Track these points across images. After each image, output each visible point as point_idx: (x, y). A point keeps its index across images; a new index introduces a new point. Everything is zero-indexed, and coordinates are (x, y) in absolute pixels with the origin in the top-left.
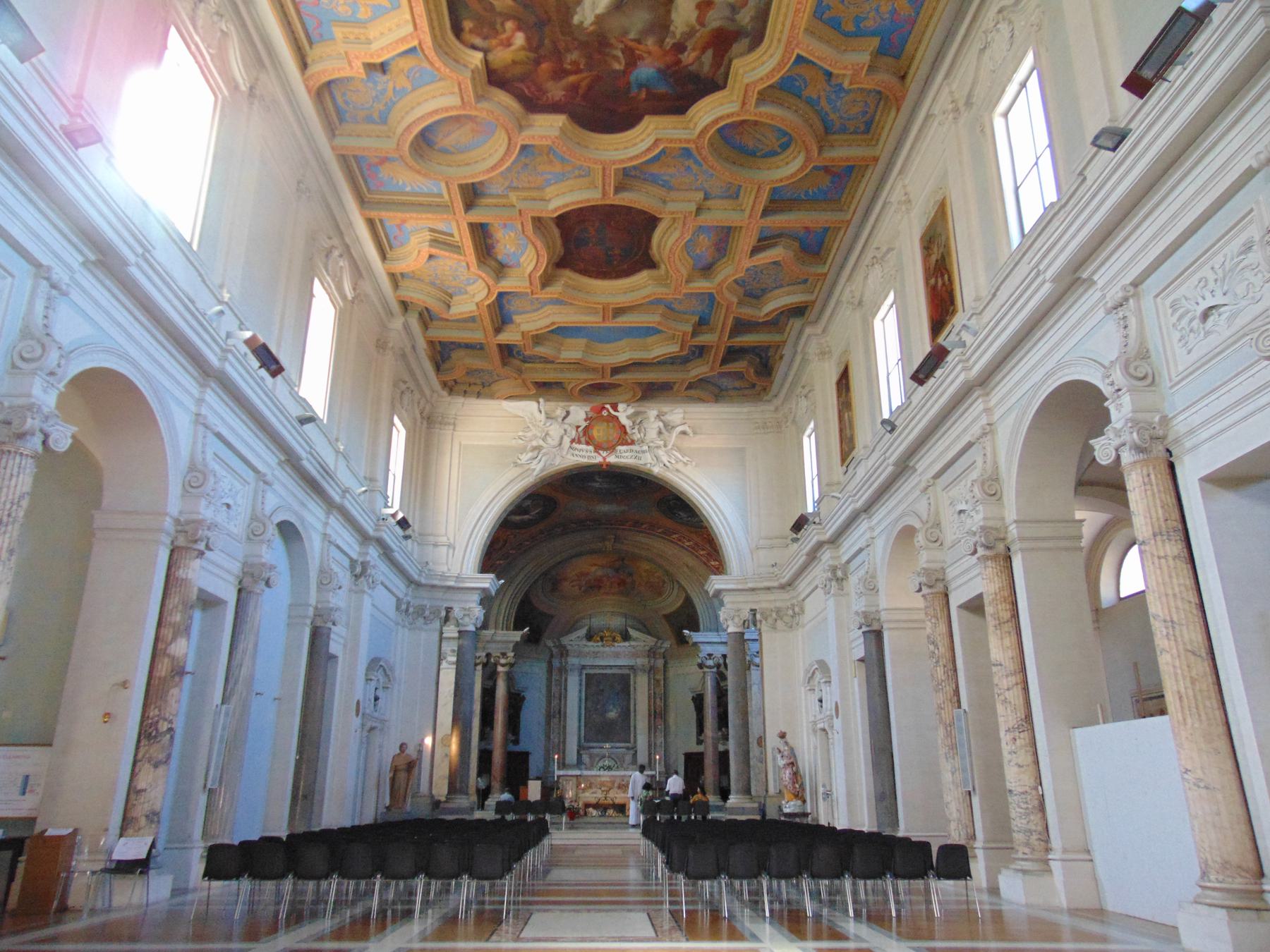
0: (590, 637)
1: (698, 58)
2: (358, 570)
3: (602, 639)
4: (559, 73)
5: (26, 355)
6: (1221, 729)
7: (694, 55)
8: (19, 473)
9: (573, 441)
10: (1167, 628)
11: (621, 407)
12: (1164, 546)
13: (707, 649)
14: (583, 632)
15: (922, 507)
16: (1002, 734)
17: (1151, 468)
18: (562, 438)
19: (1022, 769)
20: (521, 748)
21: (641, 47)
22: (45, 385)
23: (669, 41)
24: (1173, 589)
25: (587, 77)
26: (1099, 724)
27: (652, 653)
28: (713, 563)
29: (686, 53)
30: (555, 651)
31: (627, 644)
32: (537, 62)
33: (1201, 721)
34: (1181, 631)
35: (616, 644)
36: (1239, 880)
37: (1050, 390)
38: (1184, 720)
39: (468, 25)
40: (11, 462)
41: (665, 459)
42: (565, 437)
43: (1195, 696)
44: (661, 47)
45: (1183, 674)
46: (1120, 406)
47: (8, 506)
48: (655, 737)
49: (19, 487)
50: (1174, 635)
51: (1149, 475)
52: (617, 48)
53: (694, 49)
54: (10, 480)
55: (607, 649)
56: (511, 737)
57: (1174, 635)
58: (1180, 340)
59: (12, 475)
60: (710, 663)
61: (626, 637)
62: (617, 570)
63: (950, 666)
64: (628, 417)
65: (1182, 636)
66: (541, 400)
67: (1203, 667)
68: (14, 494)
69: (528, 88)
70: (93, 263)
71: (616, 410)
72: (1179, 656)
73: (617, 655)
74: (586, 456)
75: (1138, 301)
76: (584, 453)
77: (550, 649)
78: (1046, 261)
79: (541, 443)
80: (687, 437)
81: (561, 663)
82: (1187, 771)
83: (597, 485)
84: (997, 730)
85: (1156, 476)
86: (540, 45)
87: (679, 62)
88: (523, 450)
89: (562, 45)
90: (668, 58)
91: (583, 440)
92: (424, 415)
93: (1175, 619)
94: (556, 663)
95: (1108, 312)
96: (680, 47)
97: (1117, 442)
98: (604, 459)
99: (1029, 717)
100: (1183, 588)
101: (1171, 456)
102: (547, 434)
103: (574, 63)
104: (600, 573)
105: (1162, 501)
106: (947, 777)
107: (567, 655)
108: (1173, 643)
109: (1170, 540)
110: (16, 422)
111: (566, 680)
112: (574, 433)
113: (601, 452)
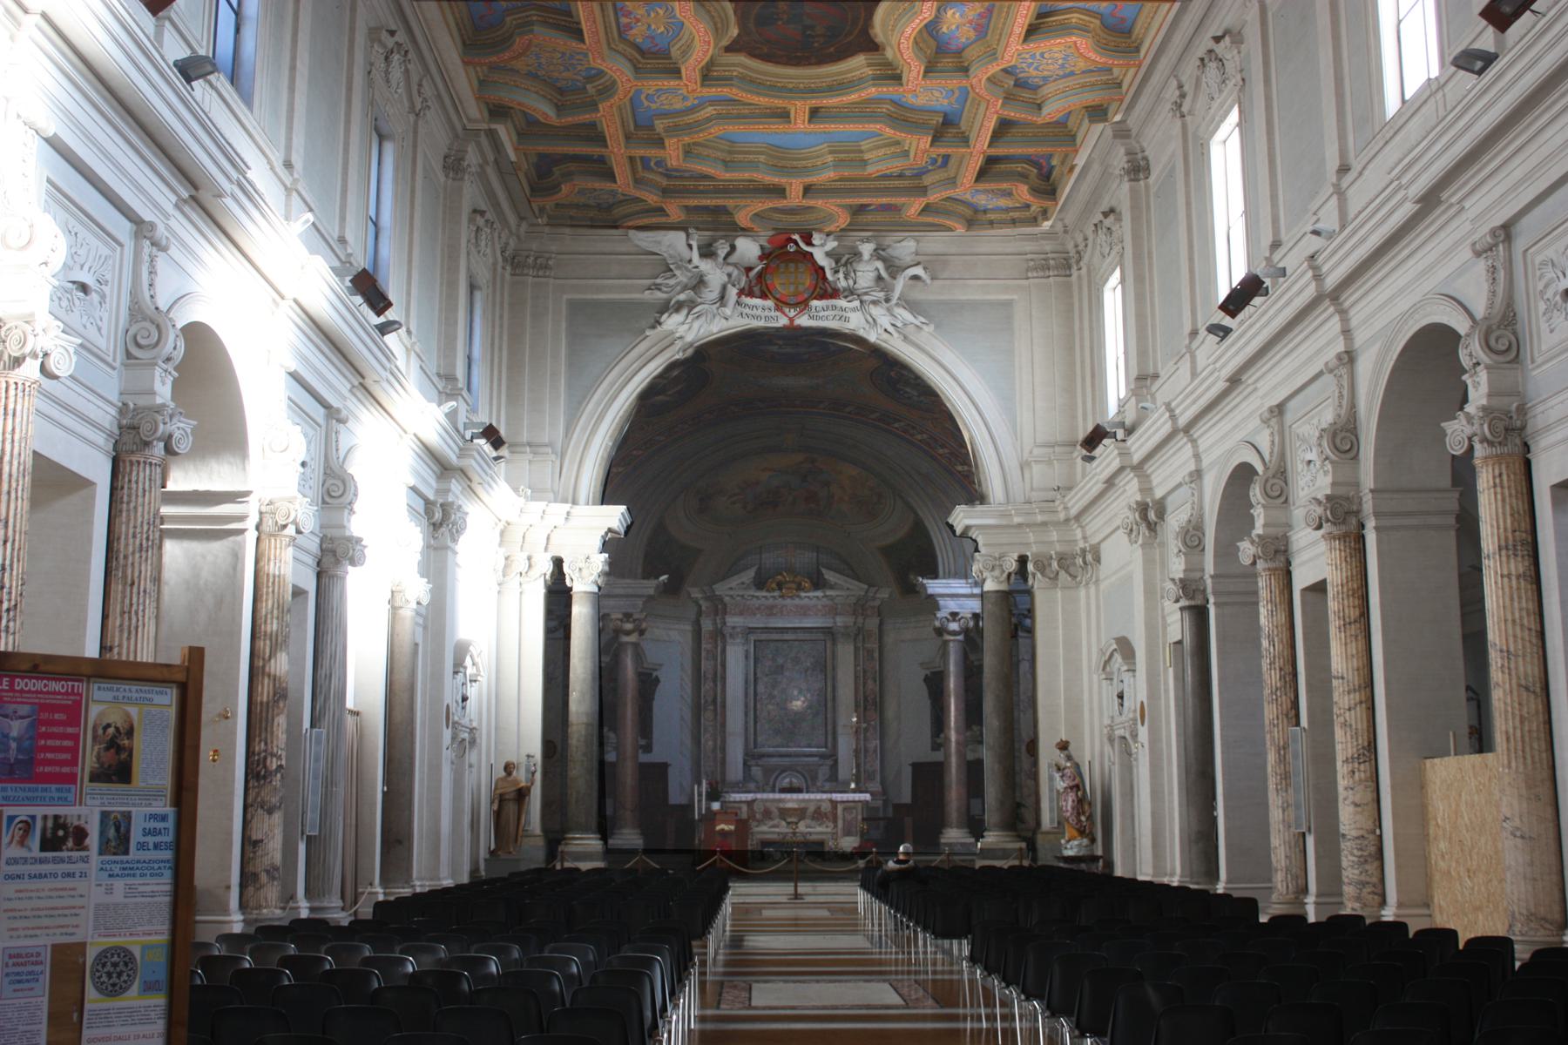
0: (760, 583)
2: (438, 515)
3: (780, 586)
5: (139, 338)
6: (1546, 774)
8: (151, 488)
9: (741, 293)
10: (1502, 658)
11: (817, 239)
12: (1508, 562)
13: (950, 606)
14: (751, 573)
15: (1264, 441)
16: (1339, 764)
17: (1503, 466)
18: (724, 288)
19: (1359, 809)
20: (656, 756)
22: (163, 375)
24: (1513, 613)
26: (1450, 755)
27: (859, 607)
28: (960, 468)
30: (704, 605)
31: (819, 593)
33: (1525, 764)
34: (1516, 662)
35: (803, 594)
36: (1542, 932)
37: (1410, 334)
38: (1509, 762)
40: (141, 475)
41: (885, 321)
42: (729, 286)
43: (1522, 737)
45: (1513, 714)
46: (1477, 385)
47: (145, 528)
48: (866, 739)
49: (152, 504)
50: (1509, 668)
51: (1500, 475)
54: (144, 495)
55: (788, 601)
56: (643, 742)
57: (1509, 668)
58: (1544, 314)
59: (144, 491)
60: (954, 626)
61: (819, 583)
63: (1288, 669)
64: (828, 254)
65: (1517, 668)
67: (1534, 704)
68: (149, 513)
70: (185, 201)
71: (809, 244)
72: (1511, 692)
73: (804, 612)
74: (761, 315)
75: (1510, 243)
76: (759, 312)
77: (696, 602)
78: (1409, 176)
80: (919, 284)
81: (715, 623)
82: (1507, 818)
83: (775, 348)
84: (1334, 759)
85: (1508, 476)
88: (665, 308)
91: (756, 290)
93: (1512, 649)
94: (707, 625)
95: (1478, 254)
97: (1468, 430)
98: (791, 320)
99: (1372, 746)
100: (1524, 614)
101: (1529, 452)
105: (1512, 507)
106: (1276, 815)
108: (1507, 676)
109: (1516, 555)
110: (145, 428)
111: (724, 651)
113: (787, 310)
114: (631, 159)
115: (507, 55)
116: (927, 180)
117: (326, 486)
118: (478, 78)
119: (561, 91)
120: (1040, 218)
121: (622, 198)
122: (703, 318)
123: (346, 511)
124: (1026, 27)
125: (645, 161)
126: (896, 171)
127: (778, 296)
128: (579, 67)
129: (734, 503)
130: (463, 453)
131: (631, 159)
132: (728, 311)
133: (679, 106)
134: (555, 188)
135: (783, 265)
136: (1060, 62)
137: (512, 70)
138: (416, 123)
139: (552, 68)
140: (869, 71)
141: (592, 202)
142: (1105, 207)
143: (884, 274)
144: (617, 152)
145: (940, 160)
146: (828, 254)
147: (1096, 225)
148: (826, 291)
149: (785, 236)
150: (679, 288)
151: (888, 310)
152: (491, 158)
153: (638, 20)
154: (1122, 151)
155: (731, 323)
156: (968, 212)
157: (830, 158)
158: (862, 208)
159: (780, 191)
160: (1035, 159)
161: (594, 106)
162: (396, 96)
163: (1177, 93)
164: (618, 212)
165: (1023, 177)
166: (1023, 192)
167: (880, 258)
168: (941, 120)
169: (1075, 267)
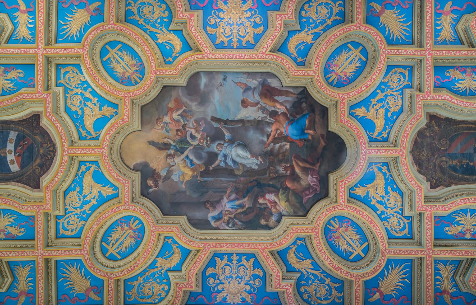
1: (281, 104)
7: (278, 106)
23: (268, 119)
25: (297, 164)
29: (278, 110)
32: (287, 188)
39: (263, 222)
44: (272, 124)
52: (274, 147)
69: (307, 195)
86: (273, 186)
87: (284, 114)
90: (281, 120)
96: (274, 114)
103: (286, 169)
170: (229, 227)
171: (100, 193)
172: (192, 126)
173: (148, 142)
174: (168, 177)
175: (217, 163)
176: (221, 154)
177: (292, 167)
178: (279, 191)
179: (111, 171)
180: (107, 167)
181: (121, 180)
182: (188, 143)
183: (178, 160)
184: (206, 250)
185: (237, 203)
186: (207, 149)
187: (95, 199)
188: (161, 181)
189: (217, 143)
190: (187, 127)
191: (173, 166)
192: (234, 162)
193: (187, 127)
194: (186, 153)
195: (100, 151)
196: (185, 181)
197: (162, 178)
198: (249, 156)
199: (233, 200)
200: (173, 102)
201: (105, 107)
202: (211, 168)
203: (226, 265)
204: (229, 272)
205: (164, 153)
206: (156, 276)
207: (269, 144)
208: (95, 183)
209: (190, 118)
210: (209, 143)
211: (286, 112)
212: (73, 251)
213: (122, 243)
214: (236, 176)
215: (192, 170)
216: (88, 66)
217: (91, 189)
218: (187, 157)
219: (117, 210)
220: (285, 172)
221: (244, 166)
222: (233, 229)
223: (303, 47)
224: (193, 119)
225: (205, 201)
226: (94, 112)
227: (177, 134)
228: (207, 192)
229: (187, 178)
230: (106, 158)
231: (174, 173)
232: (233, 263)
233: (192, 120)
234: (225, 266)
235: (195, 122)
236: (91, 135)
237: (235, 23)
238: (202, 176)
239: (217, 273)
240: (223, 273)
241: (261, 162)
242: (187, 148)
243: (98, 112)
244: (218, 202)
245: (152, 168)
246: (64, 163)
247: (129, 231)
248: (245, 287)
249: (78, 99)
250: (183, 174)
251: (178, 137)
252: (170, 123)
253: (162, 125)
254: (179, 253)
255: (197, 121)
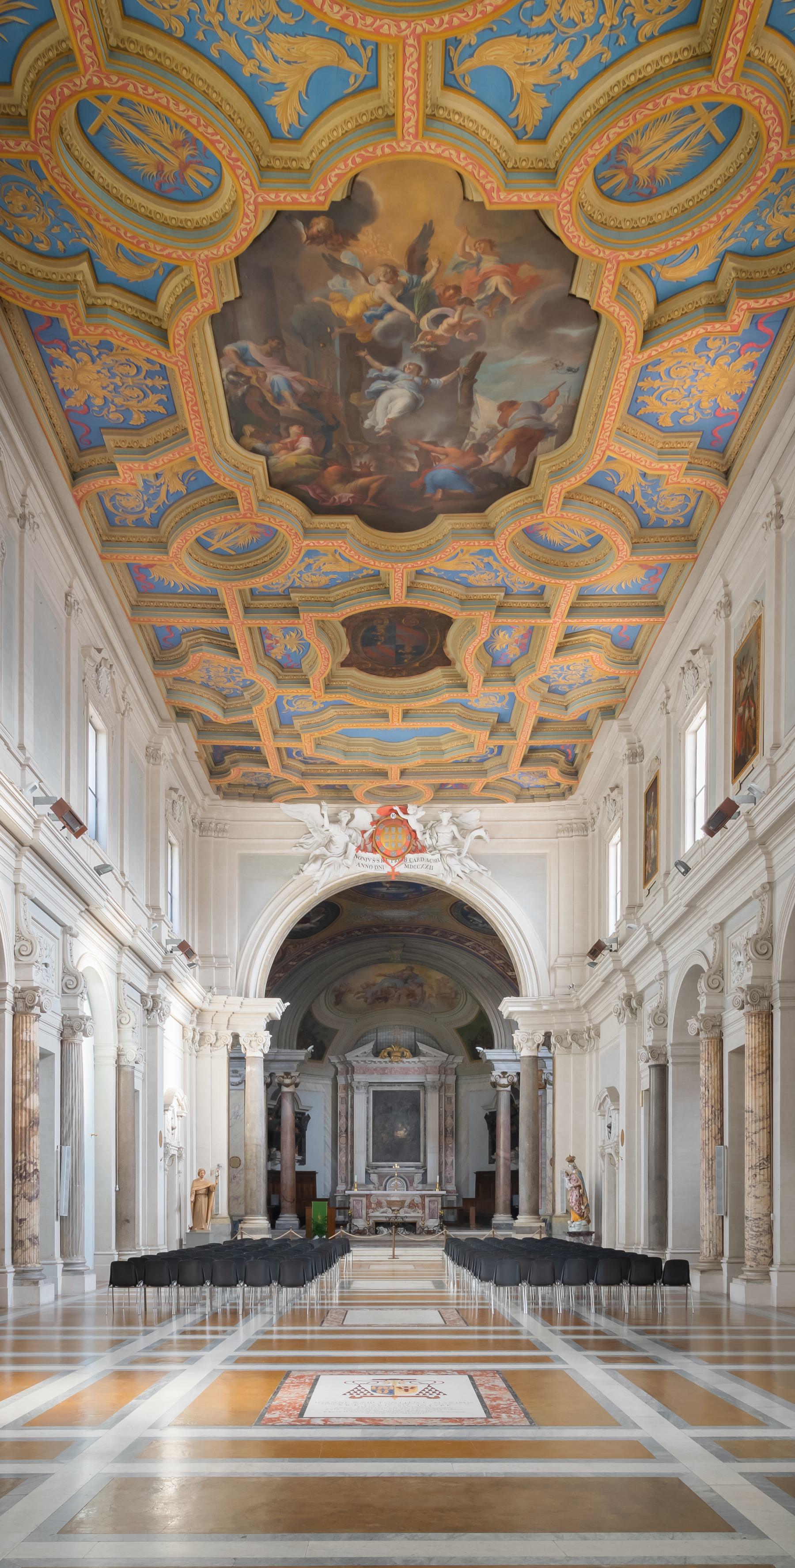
0: (376, 1053)
1: (500, 458)
3: (389, 1055)
4: (347, 477)
7: (494, 455)
9: (359, 848)
11: (411, 809)
18: (347, 845)
21: (438, 449)
23: (468, 443)
27: (442, 1070)
29: (487, 454)
30: (340, 1067)
31: (416, 1059)
32: (324, 465)
35: (405, 1060)
42: (350, 844)
44: (459, 448)
53: (495, 449)
55: (395, 1065)
61: (415, 1052)
62: (406, 981)
64: (419, 821)
66: (323, 803)
71: (405, 813)
73: (406, 1072)
76: (371, 863)
79: (322, 850)
81: (347, 1080)
83: (384, 890)
86: (328, 447)
88: (305, 860)
89: (351, 449)
91: (369, 847)
92: (196, 821)
96: (480, 448)
98: (393, 868)
102: (331, 841)
104: (386, 984)
107: (353, 1072)
112: (360, 839)
113: (389, 861)
114: (278, 749)
115: (184, 669)
116: (487, 765)
117: (65, 981)
118: (166, 687)
119: (226, 697)
120: (567, 793)
121: (274, 779)
122: (332, 867)
123: (79, 999)
124: (556, 646)
125: (289, 751)
126: (464, 758)
127: (384, 851)
128: (238, 679)
129: (359, 998)
130: (166, 960)
131: (278, 749)
132: (349, 862)
133: (310, 709)
134: (226, 772)
135: (387, 829)
136: (582, 673)
137: (190, 681)
138: (122, 720)
139: (218, 679)
140: (444, 681)
141: (254, 783)
142: (612, 785)
143: (458, 835)
144: (268, 745)
145: (496, 750)
146: (419, 821)
147: (605, 798)
148: (417, 847)
149: (389, 808)
150: (315, 846)
151: (460, 861)
152: (180, 749)
153: (277, 642)
154: (625, 741)
155: (352, 870)
156: (516, 789)
157: (418, 749)
158: (442, 787)
159: (384, 774)
160: (563, 749)
161: (249, 708)
162: (106, 699)
163: (665, 695)
164: (272, 789)
165: (555, 762)
166: (554, 774)
167: (455, 823)
168: (496, 719)
169: (590, 829)
170: (227, 374)
171: (280, 87)
172: (465, 317)
173: (431, 222)
174: (336, 266)
175: (377, 364)
176: (396, 372)
177: (369, 474)
178: (318, 456)
179: (349, 162)
180: (363, 152)
181: (325, 185)
182: (426, 311)
183: (382, 290)
184: (171, 358)
185: (286, 394)
186: (408, 348)
187: (258, 72)
188: (327, 252)
189: (423, 365)
190: (464, 308)
191: (367, 280)
192: (379, 393)
193: (464, 308)
194: (400, 307)
195: (409, 134)
196: (329, 303)
197: (335, 254)
198: (391, 416)
199: (290, 387)
200: (533, 274)
201: (544, 103)
202: (363, 354)
203: (139, 369)
204: (124, 373)
205: (399, 260)
206: (66, 225)
207: (417, 445)
208: (308, 74)
209: (486, 313)
210: (424, 350)
211: (482, 465)
212: (87, 41)
213: (136, 141)
214: (347, 394)
215: (358, 319)
216: (673, 95)
217: (288, 62)
218: (390, 309)
219: (239, 172)
220: (358, 464)
221: (371, 407)
222: (223, 381)
223: (610, 479)
224: (481, 317)
225: (284, 338)
226: (534, 68)
227: (447, 288)
228: (305, 343)
229: (336, 308)
230: (387, 150)
231: (348, 282)
232: (145, 378)
233: (481, 317)
234: (136, 366)
235: (475, 323)
236: (461, 61)
237: (694, 383)
238: (343, 336)
239: (114, 352)
240: (117, 361)
241: (379, 433)
242: (412, 309)
243: (531, 80)
244: (284, 362)
245: (359, 231)
246: (373, 24)
247: (176, 163)
248: (97, 396)
249: (582, 14)
250: (346, 300)
251: (439, 291)
252: (479, 270)
253: (474, 254)
254: (141, 277)
255: (477, 326)
